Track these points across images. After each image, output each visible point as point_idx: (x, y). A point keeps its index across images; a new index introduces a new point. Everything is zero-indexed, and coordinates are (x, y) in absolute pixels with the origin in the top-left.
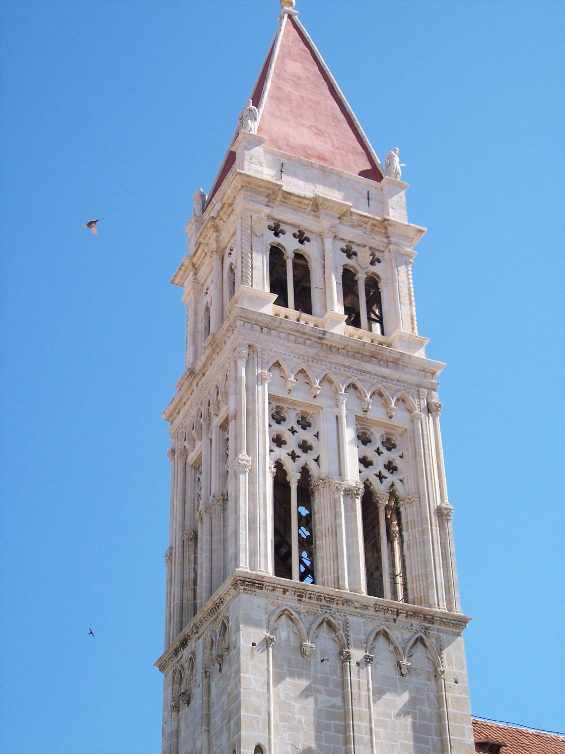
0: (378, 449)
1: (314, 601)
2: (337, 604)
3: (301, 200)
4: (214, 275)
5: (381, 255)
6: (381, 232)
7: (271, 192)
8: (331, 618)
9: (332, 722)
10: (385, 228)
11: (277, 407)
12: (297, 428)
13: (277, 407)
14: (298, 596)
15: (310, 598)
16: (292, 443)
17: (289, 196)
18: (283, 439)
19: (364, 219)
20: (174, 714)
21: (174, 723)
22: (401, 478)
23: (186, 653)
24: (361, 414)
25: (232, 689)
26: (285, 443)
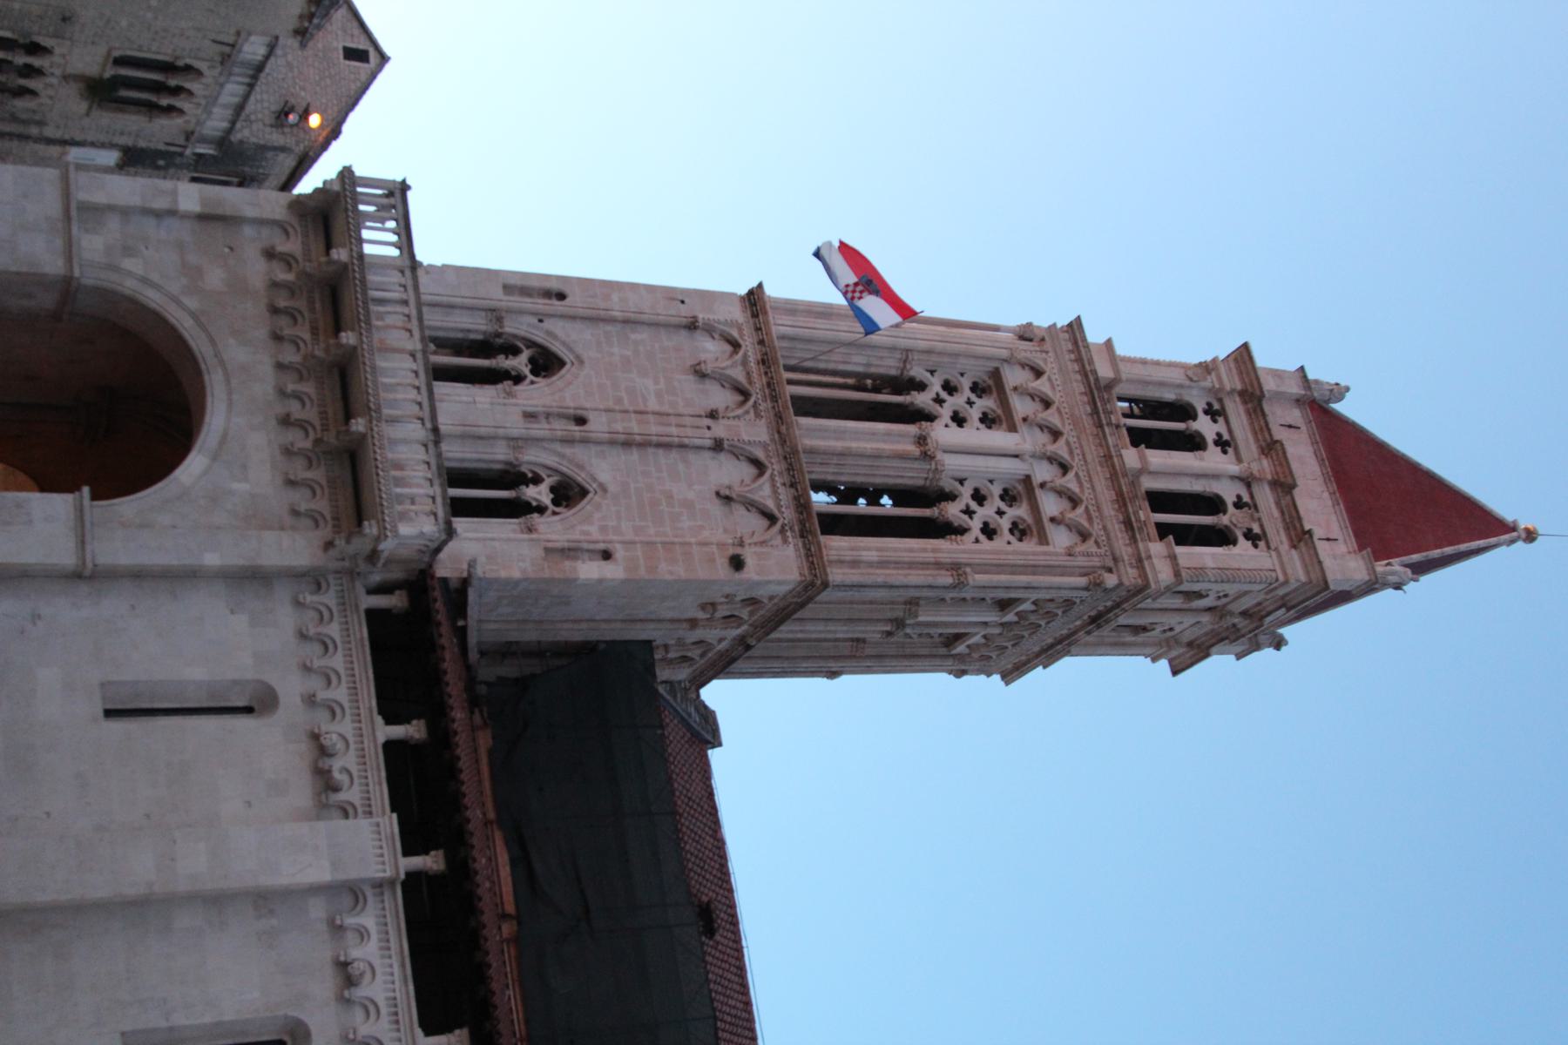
1: (764, 380)
2: (774, 407)
3: (1265, 429)
7: (1250, 390)
10: (1300, 541)
11: (989, 387)
15: (766, 373)
17: (1260, 414)
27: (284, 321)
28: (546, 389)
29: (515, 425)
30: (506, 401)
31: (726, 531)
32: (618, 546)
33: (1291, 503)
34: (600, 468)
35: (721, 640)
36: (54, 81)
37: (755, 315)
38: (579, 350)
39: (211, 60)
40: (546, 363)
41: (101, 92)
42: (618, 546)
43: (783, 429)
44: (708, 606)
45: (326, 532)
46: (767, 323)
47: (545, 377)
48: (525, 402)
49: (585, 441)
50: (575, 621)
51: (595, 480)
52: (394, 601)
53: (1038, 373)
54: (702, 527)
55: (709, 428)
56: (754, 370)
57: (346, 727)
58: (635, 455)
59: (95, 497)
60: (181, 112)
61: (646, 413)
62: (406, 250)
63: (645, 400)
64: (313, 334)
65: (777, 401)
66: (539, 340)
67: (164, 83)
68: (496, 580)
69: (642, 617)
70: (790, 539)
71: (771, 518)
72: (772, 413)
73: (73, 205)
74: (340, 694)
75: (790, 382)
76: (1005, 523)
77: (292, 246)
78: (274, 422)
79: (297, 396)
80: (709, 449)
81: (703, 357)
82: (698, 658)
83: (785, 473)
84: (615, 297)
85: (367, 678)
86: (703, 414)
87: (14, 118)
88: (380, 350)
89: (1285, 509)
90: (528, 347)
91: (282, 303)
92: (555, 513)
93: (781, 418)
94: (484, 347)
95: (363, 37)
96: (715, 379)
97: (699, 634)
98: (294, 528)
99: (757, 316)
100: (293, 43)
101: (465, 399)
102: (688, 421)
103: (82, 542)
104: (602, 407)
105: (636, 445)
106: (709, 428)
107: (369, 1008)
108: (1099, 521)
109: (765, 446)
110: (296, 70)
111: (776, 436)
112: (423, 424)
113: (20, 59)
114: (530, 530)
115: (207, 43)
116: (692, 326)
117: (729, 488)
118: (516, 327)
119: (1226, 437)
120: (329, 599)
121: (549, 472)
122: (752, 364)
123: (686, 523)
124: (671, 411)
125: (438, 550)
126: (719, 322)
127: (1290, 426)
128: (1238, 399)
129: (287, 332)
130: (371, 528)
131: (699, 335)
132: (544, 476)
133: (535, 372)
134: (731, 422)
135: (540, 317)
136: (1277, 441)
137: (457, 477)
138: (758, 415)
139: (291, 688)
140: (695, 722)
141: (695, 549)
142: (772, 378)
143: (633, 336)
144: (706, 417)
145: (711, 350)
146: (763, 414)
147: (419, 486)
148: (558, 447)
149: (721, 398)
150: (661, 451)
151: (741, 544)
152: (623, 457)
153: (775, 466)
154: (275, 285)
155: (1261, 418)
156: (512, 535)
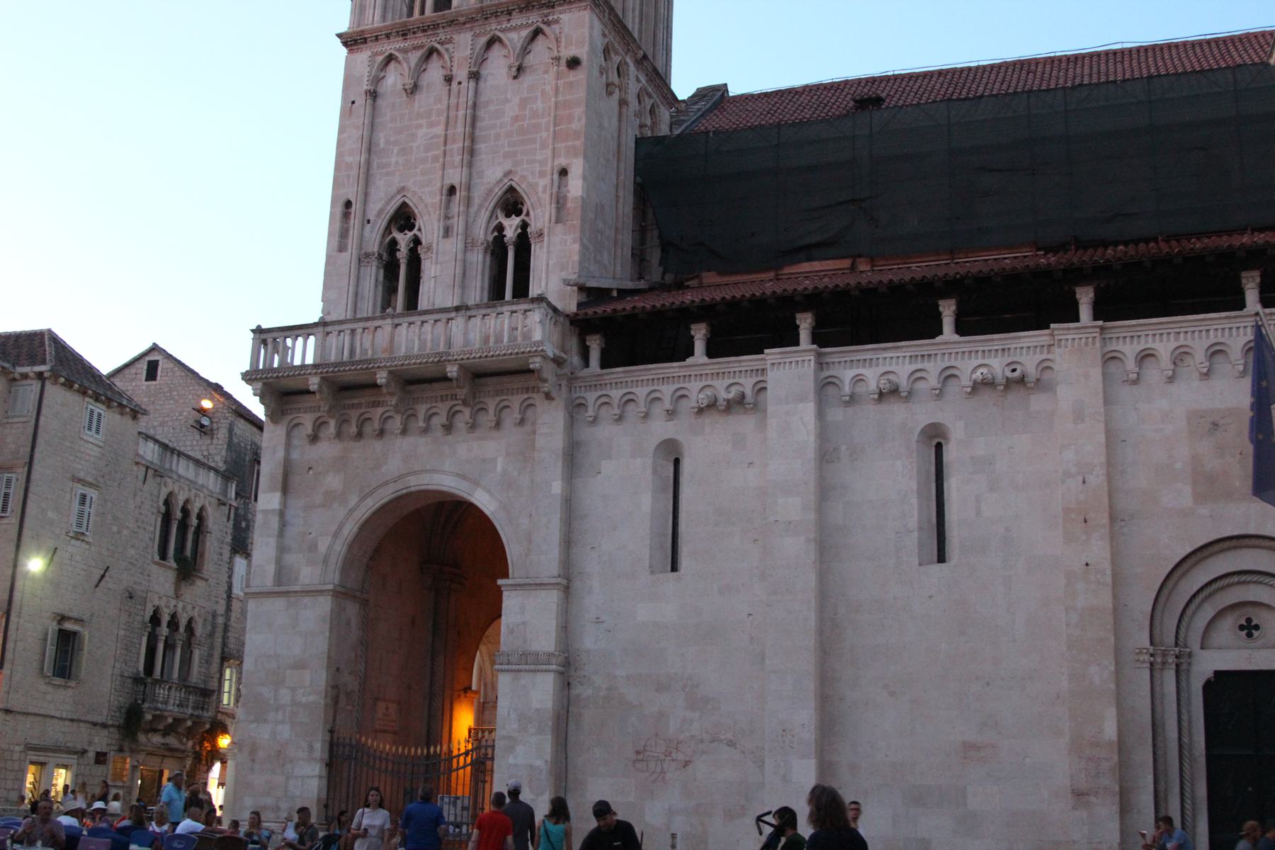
1: (420, 34)
2: (443, 27)
9: (430, 154)
14: (403, 35)
15: (414, 33)
27: (368, 429)
28: (425, 219)
29: (452, 246)
30: (434, 252)
31: (546, 72)
32: (556, 162)
34: (491, 175)
35: (638, 80)
36: (180, 605)
37: (365, 41)
38: (393, 190)
39: (159, 484)
40: (404, 218)
41: (188, 569)
42: (556, 162)
43: (462, 19)
44: (609, 89)
45: (538, 399)
46: (372, 31)
47: (415, 219)
48: (435, 235)
49: (469, 189)
50: (617, 202)
51: (501, 180)
52: (595, 345)
54: (543, 92)
55: (460, 83)
56: (411, 43)
57: (694, 386)
58: (481, 147)
59: (506, 576)
60: (202, 509)
61: (446, 136)
62: (310, 331)
63: (436, 136)
64: (378, 406)
65: (438, 24)
66: (384, 224)
67: (179, 521)
68: (580, 263)
69: (616, 147)
70: (555, 17)
71: (537, 32)
72: (448, 29)
73: (277, 589)
74: (667, 390)
75: (422, 12)
77: (307, 421)
78: (449, 438)
79: (428, 418)
80: (477, 84)
81: (400, 87)
82: (652, 101)
83: (499, 19)
84: (349, 159)
85: (654, 369)
86: (448, 87)
87: (211, 635)
88: (391, 351)
90: (391, 233)
91: (353, 429)
92: (528, 214)
93: (452, 21)
94: (390, 268)
95: (137, 365)
96: (418, 77)
97: (632, 98)
98: (534, 424)
99: (365, 39)
100: (143, 420)
101: (432, 285)
102: (453, 100)
103: (541, 585)
104: (440, 173)
105: (473, 145)
106: (460, 83)
107: (916, 375)
109: (476, 36)
110: (166, 419)
111: (467, 26)
112: (452, 319)
113: (164, 630)
114: (541, 235)
115: (146, 488)
116: (373, 95)
117: (510, 67)
118: (373, 240)
120: (591, 397)
121: (494, 218)
122: (406, 45)
123: (539, 105)
124: (445, 115)
125: (555, 310)
129: (377, 426)
130: (535, 363)
131: (381, 90)
132: (498, 221)
133: (411, 227)
134: (455, 64)
135: (366, 222)
137: (496, 293)
138: (450, 41)
139: (661, 429)
140: (705, 105)
141: (560, 98)
142: (418, 28)
143: (382, 145)
144: (450, 85)
145: (394, 79)
146: (448, 37)
147: (502, 323)
148: (473, 209)
149: (434, 73)
150: (479, 124)
151: (558, 59)
152: (483, 156)
153: (493, 27)
154: (339, 435)
156: (545, 250)
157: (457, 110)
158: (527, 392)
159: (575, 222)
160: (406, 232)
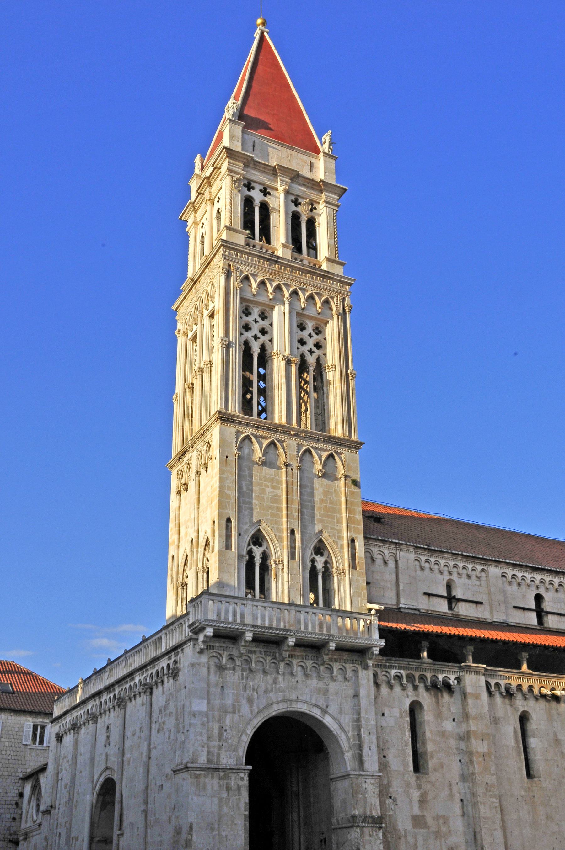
0: (310, 334)
2: (280, 432)
3: (265, 167)
4: (208, 215)
5: (318, 205)
6: (317, 189)
8: (276, 441)
9: (275, 505)
11: (246, 306)
12: (259, 319)
13: (246, 306)
16: (255, 330)
17: (258, 164)
18: (249, 326)
19: (307, 180)
20: (178, 497)
21: (178, 502)
22: (324, 353)
23: (186, 459)
24: (300, 311)
25: (213, 484)
26: (250, 329)
33: (304, 179)
37: (233, 422)
53: (247, 278)
65: (279, 429)
73: (208, 766)
76: (315, 337)
89: (304, 183)
99: (234, 420)
108: (321, 291)
119: (262, 187)
126: (237, 441)
127: (254, 146)
128: (246, 169)
132: (312, 557)
133: (260, 545)
136: (275, 166)
144: (287, 469)
155: (260, 165)
157: (293, 486)
158: (353, 663)
159: (363, 571)
160: (257, 546)
